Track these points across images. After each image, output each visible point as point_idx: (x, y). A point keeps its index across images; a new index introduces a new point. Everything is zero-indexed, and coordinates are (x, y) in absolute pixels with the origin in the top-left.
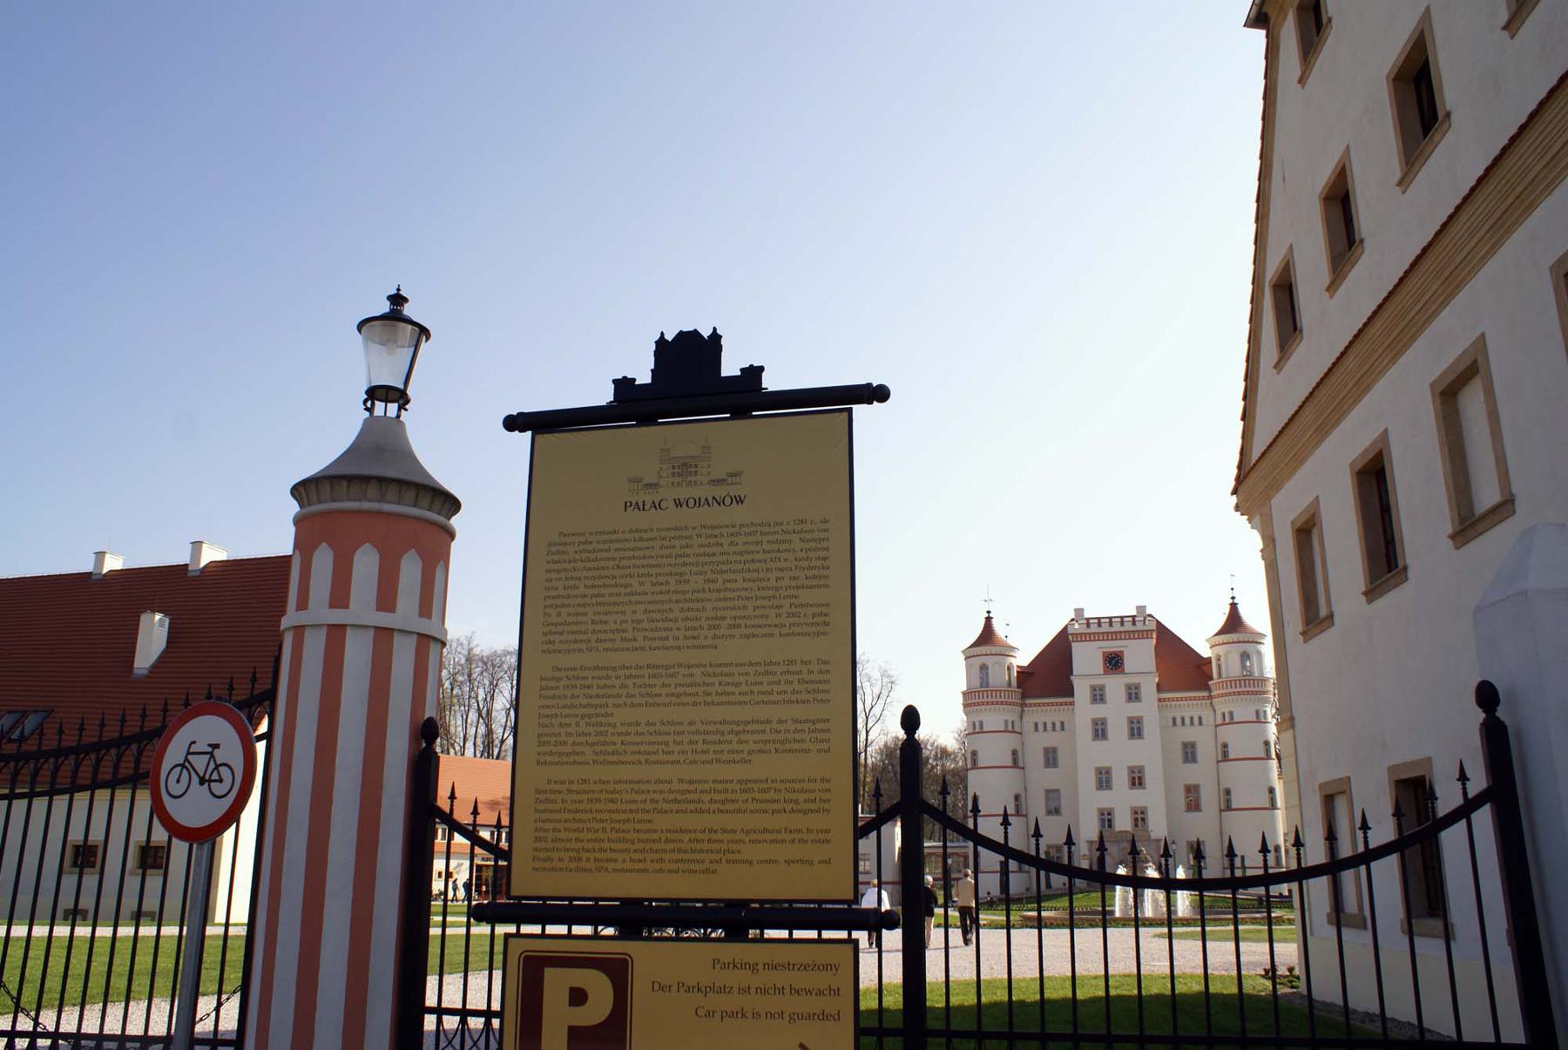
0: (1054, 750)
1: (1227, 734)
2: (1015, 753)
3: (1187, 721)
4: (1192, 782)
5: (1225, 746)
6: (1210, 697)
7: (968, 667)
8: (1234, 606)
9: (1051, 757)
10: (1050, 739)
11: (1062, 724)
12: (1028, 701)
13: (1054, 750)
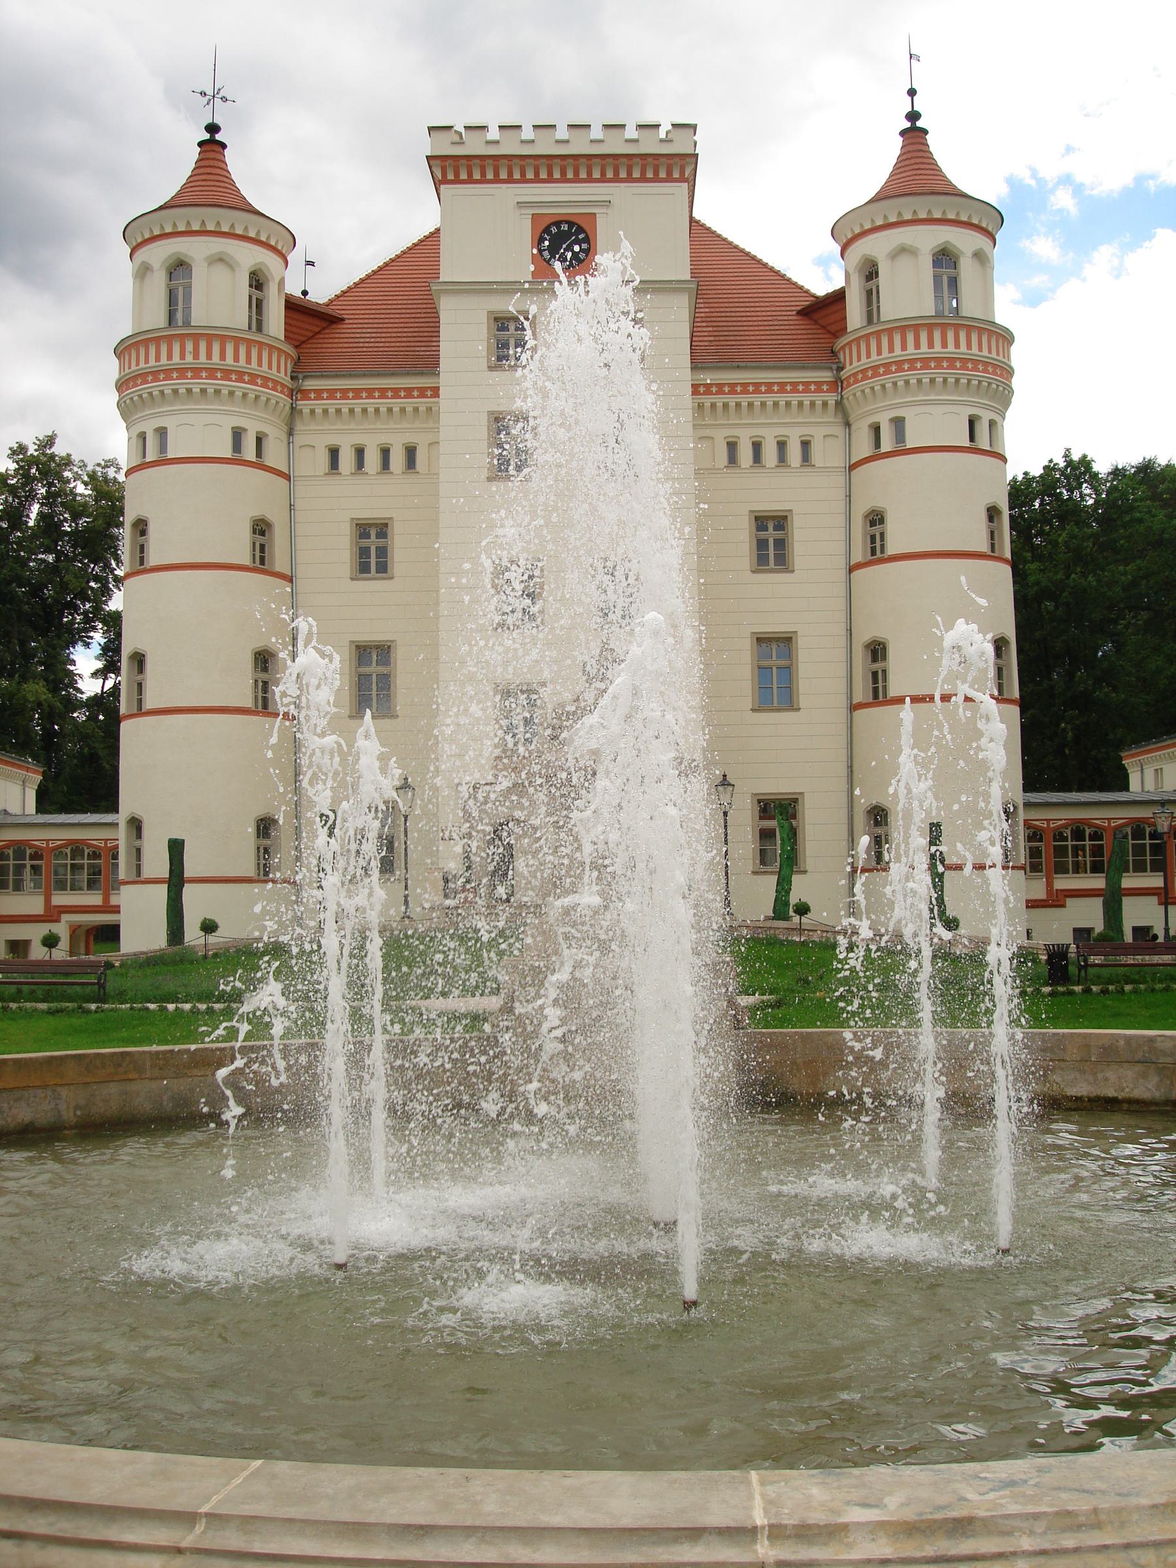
0: (383, 529)
1: (886, 484)
2: (261, 528)
3: (770, 453)
4: (775, 625)
5: (876, 519)
6: (838, 384)
7: (143, 272)
8: (914, 134)
9: (372, 549)
10: (371, 496)
11: (411, 453)
12: (310, 384)
13: (383, 529)
